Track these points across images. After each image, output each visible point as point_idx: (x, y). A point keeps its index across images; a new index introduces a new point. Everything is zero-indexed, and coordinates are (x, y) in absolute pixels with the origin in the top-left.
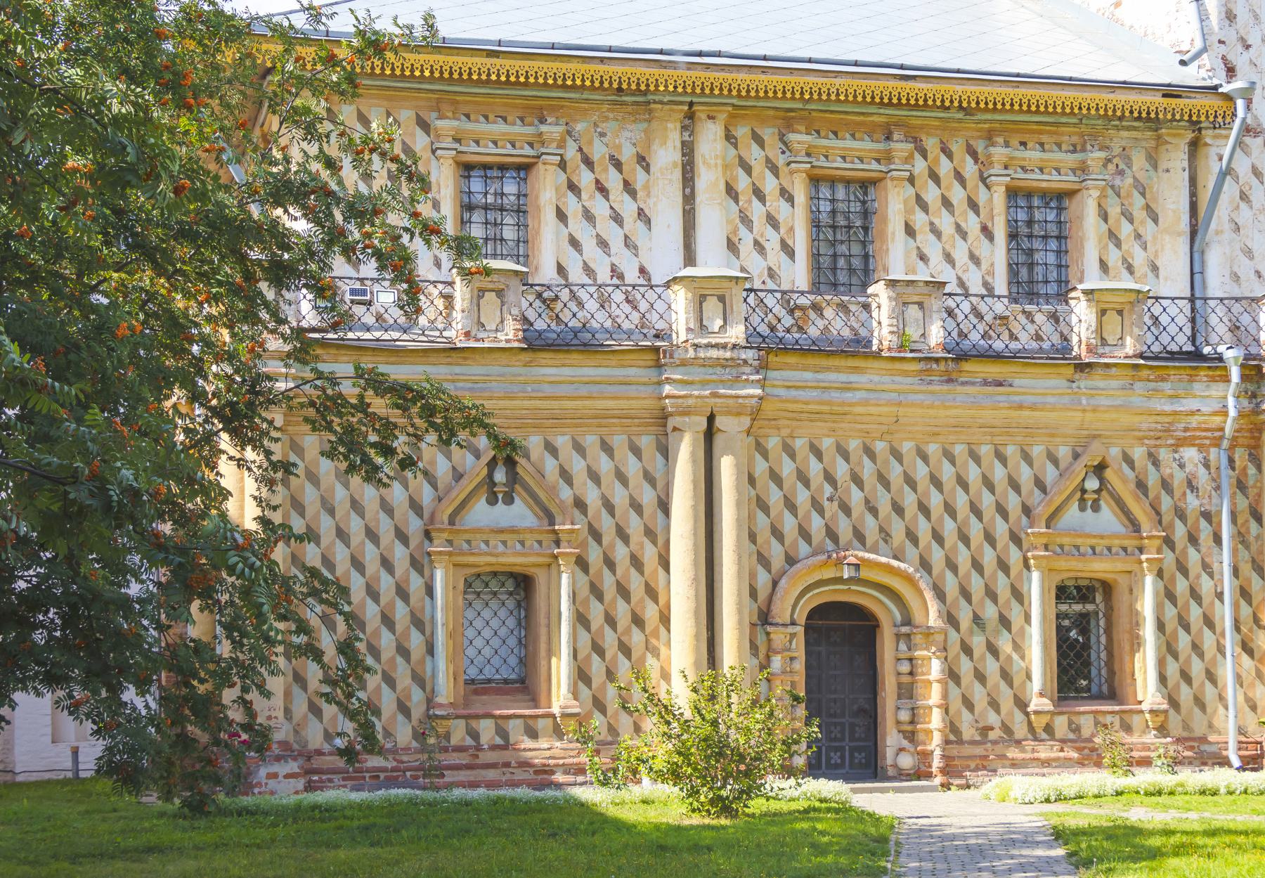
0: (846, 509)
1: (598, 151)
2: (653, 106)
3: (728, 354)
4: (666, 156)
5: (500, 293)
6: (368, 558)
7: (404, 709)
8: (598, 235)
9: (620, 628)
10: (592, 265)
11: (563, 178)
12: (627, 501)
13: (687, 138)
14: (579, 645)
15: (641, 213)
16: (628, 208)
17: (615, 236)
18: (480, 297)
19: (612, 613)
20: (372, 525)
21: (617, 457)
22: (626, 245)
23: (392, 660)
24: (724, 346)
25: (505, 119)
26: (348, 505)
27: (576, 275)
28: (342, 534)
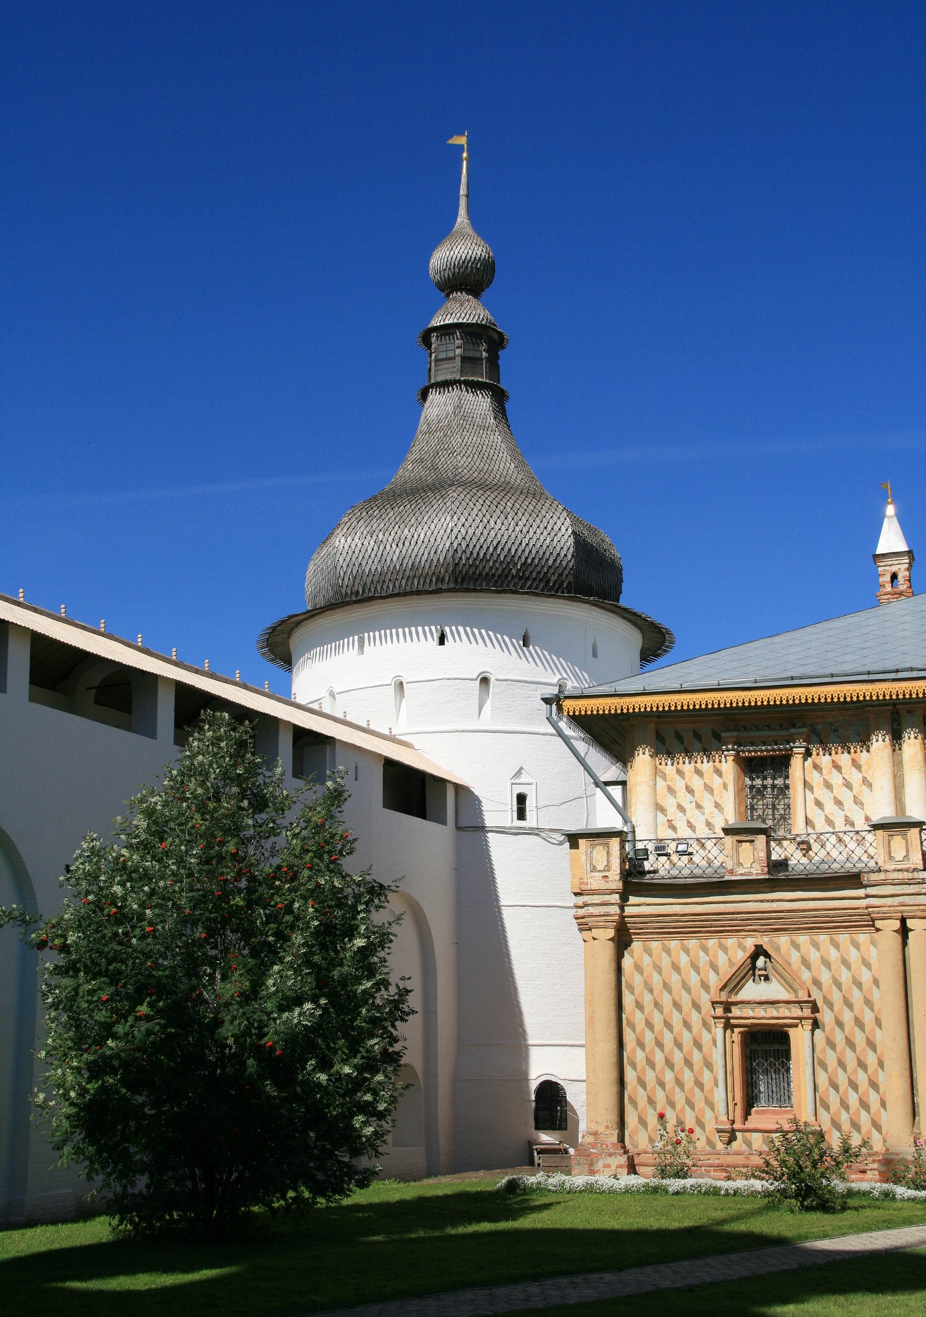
3: (910, 875)
8: (835, 797)
9: (849, 1070)
12: (851, 980)
13: (896, 727)
14: (818, 1082)
15: (865, 780)
16: (855, 777)
17: (846, 797)
18: (737, 847)
20: (677, 999)
22: (855, 802)
24: (907, 870)
27: (821, 825)
28: (657, 1005)
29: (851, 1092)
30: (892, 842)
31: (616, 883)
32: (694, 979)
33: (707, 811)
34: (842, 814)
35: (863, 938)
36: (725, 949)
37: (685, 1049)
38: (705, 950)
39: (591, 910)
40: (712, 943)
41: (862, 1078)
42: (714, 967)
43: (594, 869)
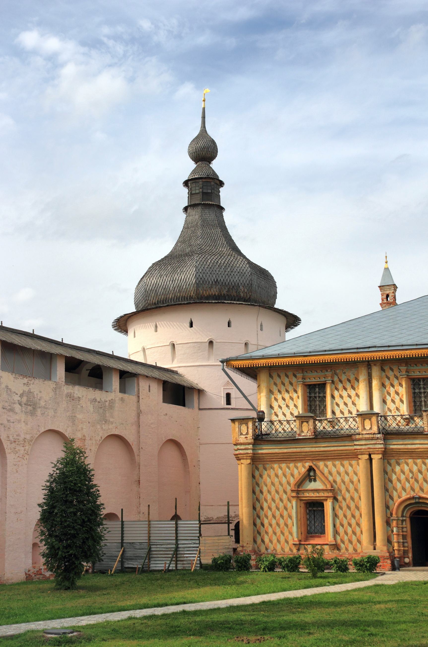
0: (417, 481)
1: (344, 378)
2: (357, 364)
3: (372, 436)
4: (363, 377)
5: (307, 422)
6: (268, 498)
7: (287, 542)
9: (348, 518)
10: (342, 410)
11: (333, 386)
12: (349, 480)
18: (302, 424)
19: (346, 514)
20: (277, 489)
21: (345, 467)
23: (283, 528)
24: (371, 434)
25: (317, 371)
26: (271, 483)
27: (338, 415)
29: (349, 528)
30: (365, 422)
31: (251, 440)
32: (284, 480)
33: (291, 408)
34: (347, 409)
35: (354, 462)
36: (297, 468)
37: (281, 510)
38: (289, 468)
39: (241, 452)
40: (292, 465)
41: (353, 522)
42: (292, 475)
43: (241, 434)
